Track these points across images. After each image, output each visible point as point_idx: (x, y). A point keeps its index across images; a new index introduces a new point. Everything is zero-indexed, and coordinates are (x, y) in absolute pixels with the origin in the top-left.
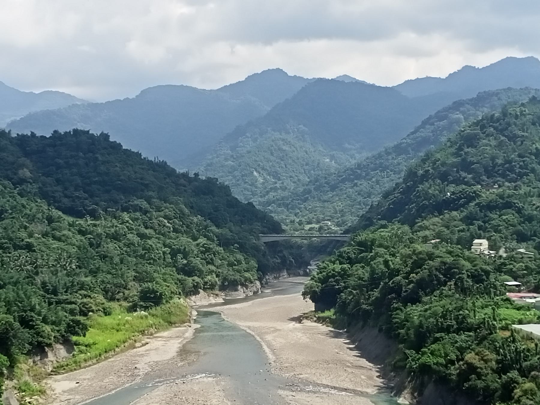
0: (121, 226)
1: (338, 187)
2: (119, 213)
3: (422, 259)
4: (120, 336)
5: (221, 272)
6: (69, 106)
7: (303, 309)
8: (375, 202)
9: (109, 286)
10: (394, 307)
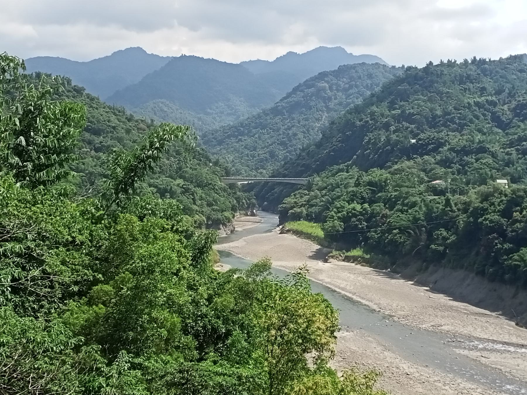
1: (224, 142)
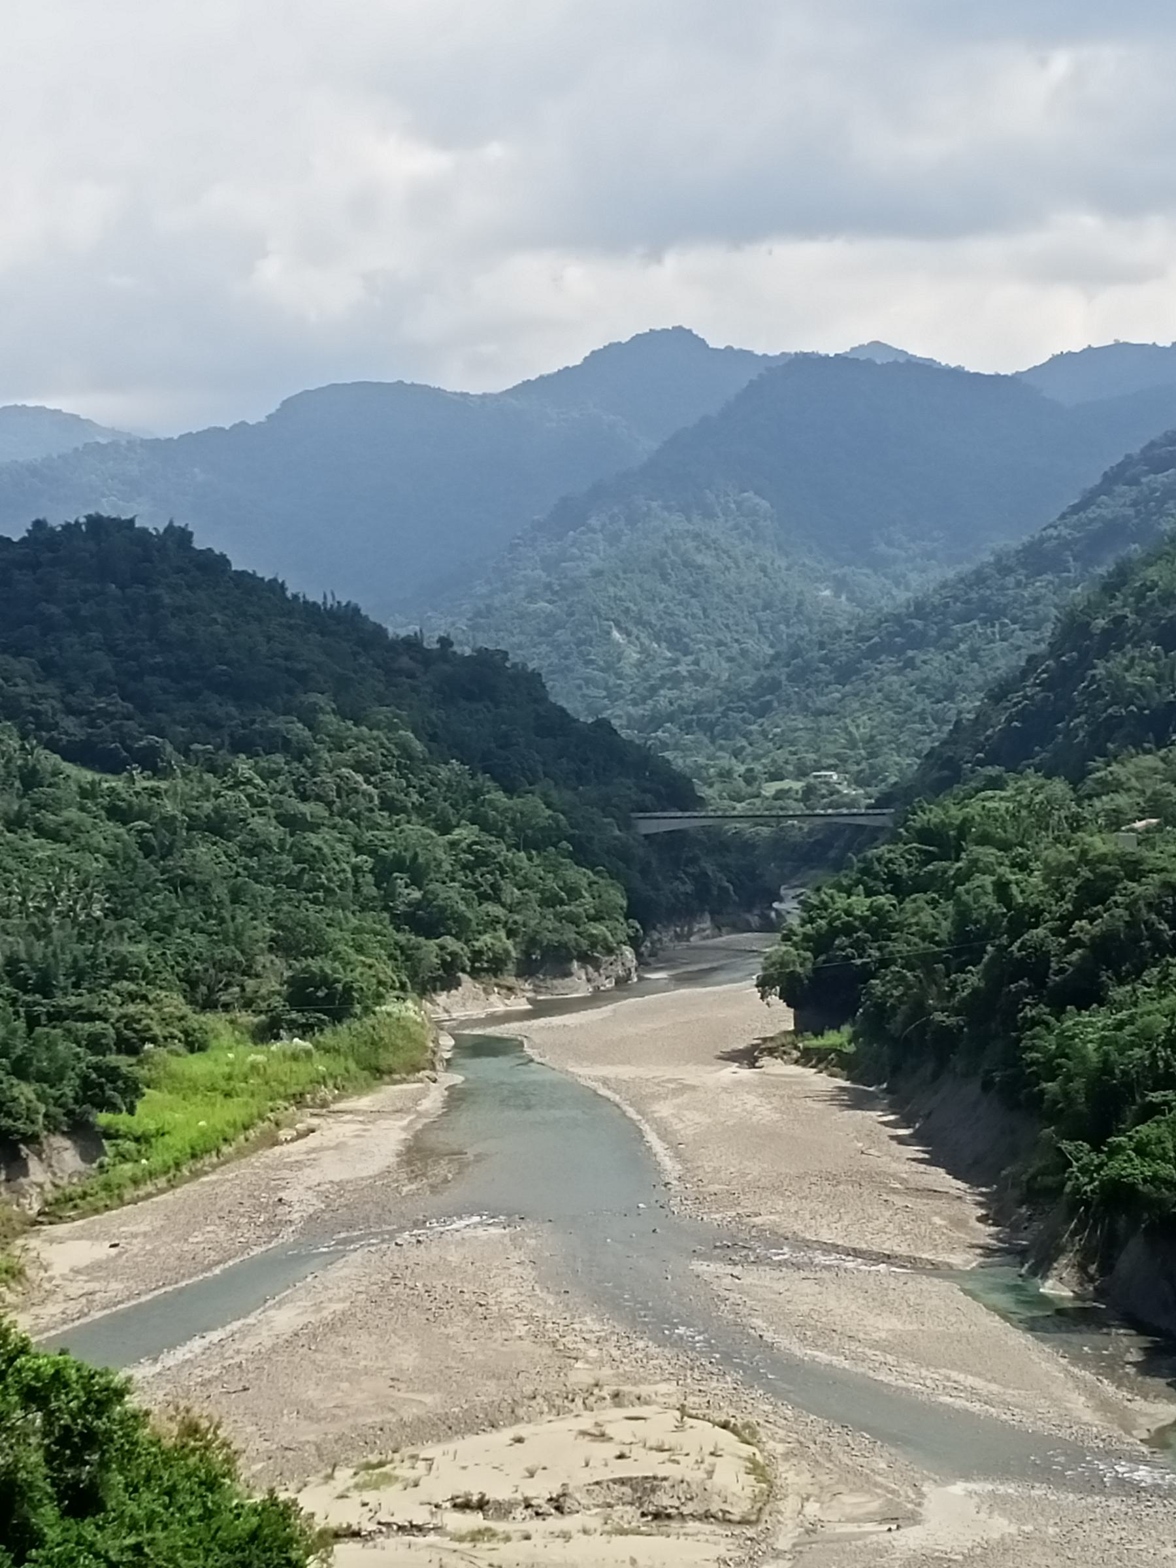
0: (230, 793)
1: (857, 672)
2: (223, 756)
3: (1106, 876)
4: (234, 1110)
5: (521, 922)
6: (76, 449)
7: (759, 1025)
8: (969, 712)
9: (198, 967)
10: (1025, 1018)
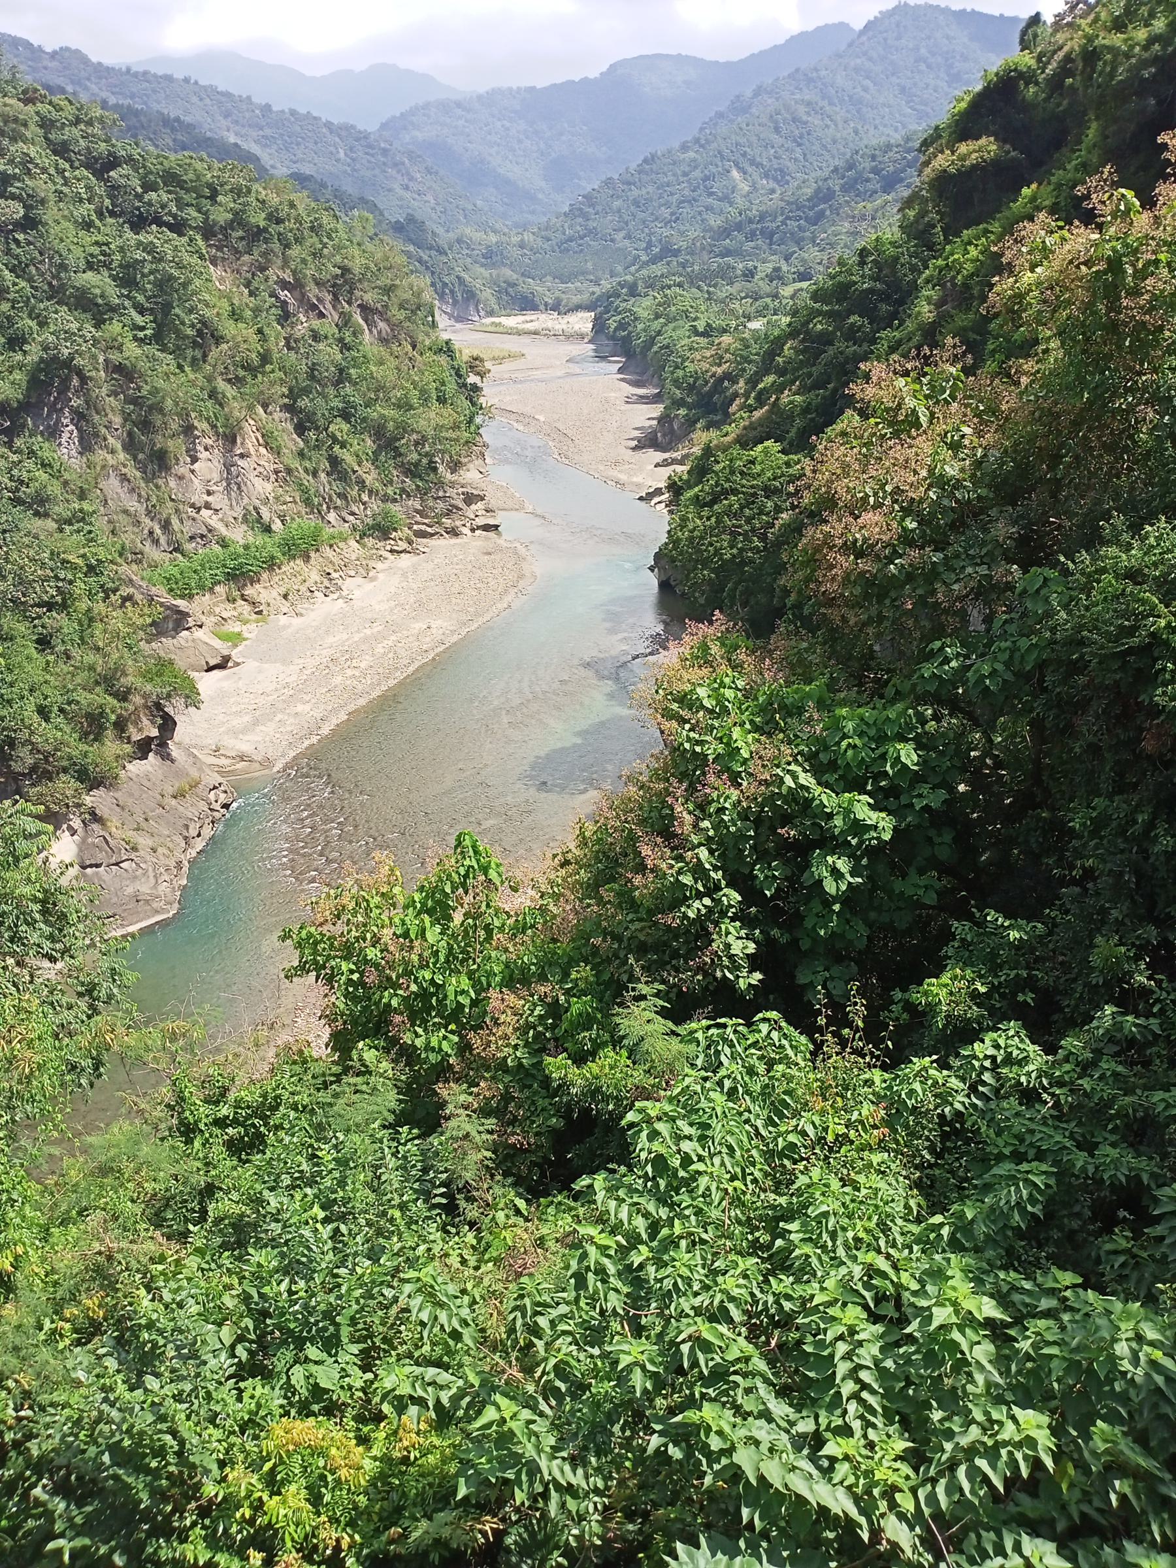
1: (902, 180)
